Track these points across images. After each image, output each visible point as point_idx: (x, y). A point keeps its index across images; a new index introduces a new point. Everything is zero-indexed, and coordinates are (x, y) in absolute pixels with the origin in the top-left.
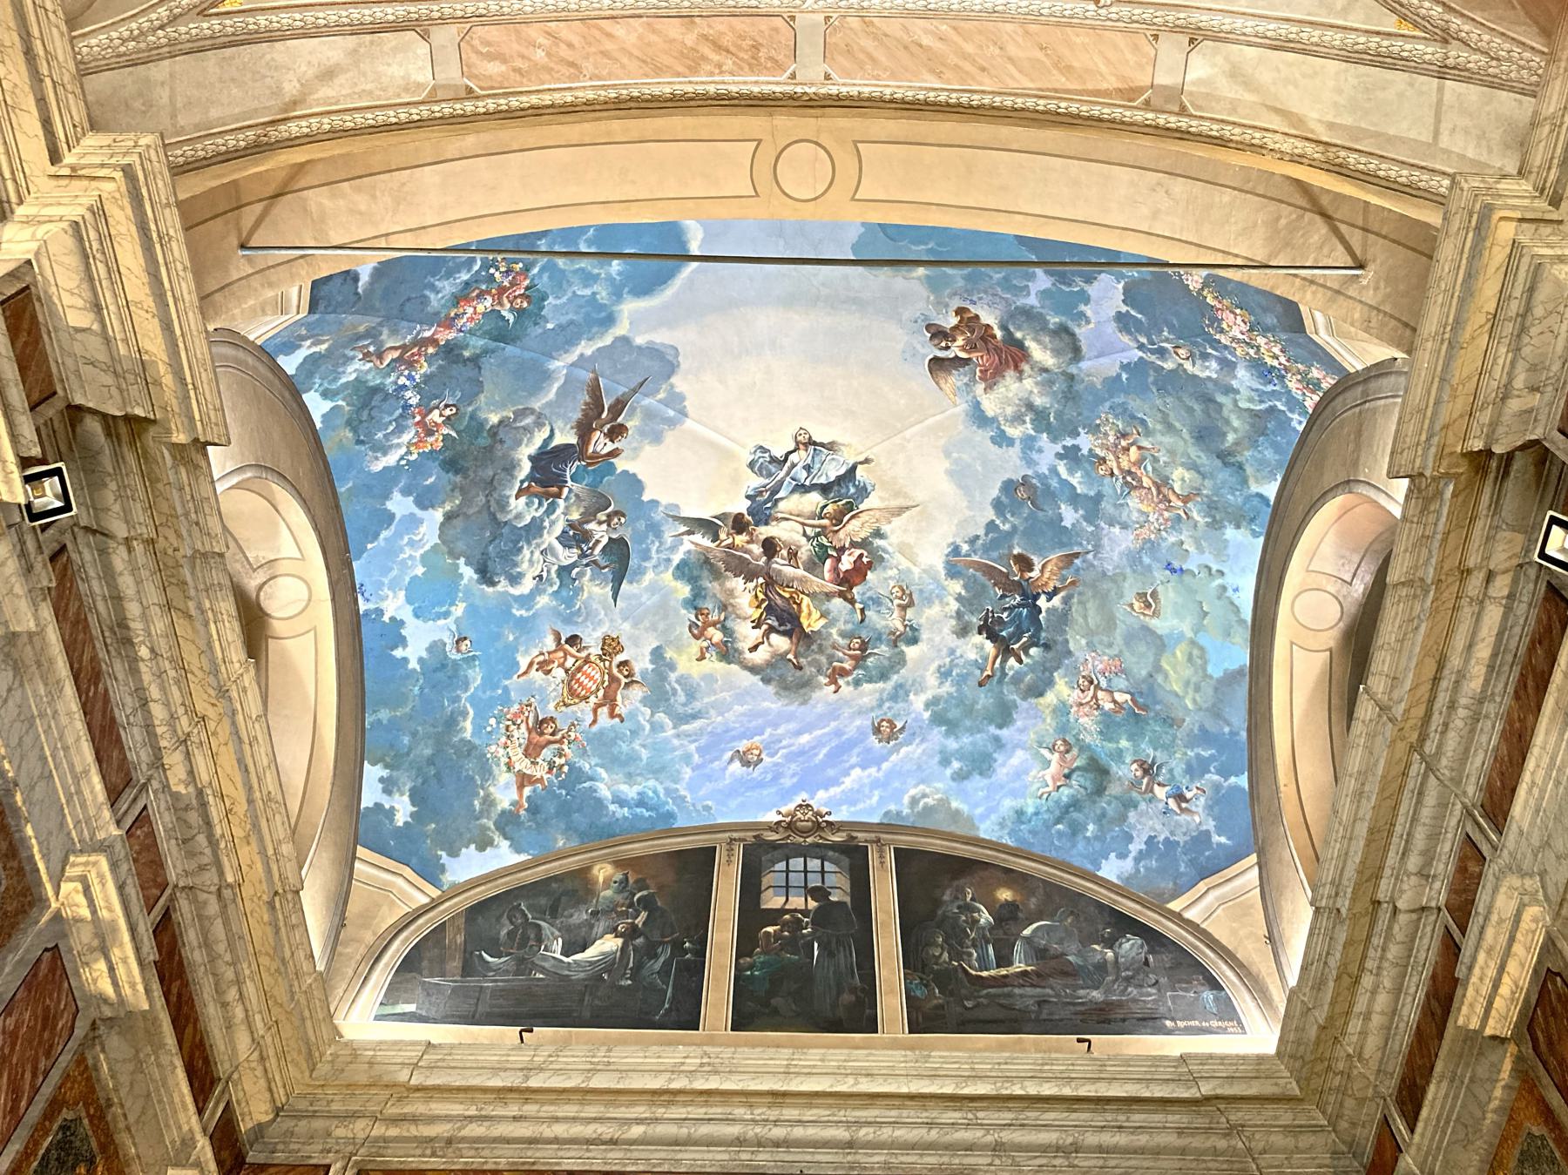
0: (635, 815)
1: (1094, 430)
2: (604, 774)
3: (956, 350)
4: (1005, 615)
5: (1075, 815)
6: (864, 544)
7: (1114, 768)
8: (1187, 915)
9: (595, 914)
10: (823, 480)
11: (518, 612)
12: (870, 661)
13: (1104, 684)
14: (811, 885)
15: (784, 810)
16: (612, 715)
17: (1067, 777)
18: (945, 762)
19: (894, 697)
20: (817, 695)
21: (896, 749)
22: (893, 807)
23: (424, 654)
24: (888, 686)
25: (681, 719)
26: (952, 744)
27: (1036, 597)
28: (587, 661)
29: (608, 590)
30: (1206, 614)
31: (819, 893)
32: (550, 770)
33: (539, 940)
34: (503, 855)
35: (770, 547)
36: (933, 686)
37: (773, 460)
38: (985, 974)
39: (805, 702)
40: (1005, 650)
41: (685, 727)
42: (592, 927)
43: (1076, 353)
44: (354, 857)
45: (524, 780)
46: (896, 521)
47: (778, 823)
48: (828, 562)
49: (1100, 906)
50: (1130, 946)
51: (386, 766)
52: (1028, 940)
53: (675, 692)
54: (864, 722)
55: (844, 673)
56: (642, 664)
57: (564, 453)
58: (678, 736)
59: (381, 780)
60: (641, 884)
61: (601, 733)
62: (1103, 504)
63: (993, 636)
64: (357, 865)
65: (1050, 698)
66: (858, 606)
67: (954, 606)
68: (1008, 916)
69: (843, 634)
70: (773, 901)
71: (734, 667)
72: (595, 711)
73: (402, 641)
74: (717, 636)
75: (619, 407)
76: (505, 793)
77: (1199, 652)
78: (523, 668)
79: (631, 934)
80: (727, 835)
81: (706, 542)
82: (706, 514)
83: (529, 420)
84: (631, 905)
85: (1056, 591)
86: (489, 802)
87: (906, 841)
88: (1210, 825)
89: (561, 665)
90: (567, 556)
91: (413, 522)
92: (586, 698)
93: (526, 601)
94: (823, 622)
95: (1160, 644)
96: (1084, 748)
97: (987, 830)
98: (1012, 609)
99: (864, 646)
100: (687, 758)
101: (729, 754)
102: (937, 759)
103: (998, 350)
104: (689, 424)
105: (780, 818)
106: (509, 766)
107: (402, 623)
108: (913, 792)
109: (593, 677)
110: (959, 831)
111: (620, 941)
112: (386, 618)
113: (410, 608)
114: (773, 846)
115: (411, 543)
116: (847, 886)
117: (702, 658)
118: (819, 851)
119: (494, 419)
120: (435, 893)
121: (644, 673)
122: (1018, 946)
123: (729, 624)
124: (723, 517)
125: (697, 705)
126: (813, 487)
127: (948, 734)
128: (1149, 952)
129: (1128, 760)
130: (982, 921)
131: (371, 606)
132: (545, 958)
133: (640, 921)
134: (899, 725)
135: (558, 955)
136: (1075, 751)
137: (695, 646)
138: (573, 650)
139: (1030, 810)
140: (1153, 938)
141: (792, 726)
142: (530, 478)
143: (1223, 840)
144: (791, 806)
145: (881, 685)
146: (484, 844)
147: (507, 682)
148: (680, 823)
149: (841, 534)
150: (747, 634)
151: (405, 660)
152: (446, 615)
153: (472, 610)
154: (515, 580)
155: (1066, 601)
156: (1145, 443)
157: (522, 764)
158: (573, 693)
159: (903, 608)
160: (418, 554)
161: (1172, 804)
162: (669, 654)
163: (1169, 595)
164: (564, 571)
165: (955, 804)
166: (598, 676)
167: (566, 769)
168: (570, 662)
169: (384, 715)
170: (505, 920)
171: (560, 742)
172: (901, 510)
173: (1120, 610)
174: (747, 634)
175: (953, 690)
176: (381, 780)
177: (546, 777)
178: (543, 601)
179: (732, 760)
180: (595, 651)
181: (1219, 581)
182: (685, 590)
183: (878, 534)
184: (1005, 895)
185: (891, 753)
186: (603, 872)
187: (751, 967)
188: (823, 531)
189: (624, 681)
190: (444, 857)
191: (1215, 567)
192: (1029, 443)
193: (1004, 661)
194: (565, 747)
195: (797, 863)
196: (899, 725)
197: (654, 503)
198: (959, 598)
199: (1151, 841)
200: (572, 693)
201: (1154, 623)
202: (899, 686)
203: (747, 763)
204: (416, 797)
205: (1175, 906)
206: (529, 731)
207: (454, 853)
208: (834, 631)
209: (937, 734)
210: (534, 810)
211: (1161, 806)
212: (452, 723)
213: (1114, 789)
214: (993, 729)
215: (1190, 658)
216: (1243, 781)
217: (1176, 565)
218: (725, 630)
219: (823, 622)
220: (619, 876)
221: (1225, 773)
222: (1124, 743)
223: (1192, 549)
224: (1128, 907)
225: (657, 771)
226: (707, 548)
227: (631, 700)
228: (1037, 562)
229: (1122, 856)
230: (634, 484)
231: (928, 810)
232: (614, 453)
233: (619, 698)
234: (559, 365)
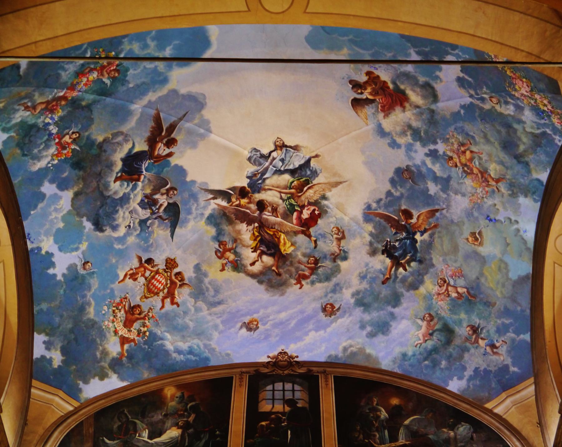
0: (187, 360)
1: (446, 141)
2: (168, 335)
3: (366, 95)
4: (397, 244)
5: (435, 356)
6: (316, 203)
7: (457, 329)
8: (496, 411)
9: (166, 416)
10: (291, 167)
11: (118, 246)
12: (320, 271)
13: (452, 283)
14: (287, 398)
15: (271, 355)
16: (173, 303)
17: (431, 335)
18: (363, 327)
19: (334, 291)
21: (335, 320)
22: (333, 353)
23: (65, 271)
24: (329, 285)
26: (367, 317)
27: (415, 234)
28: (157, 272)
29: (168, 232)
30: (508, 245)
31: (291, 402)
32: (138, 335)
33: (135, 431)
35: (261, 206)
36: (356, 284)
37: (262, 156)
39: (282, 294)
40: (397, 263)
41: (214, 310)
42: (164, 423)
43: (435, 97)
44: (31, 386)
45: (124, 340)
46: (334, 190)
47: (268, 363)
48: (295, 214)
49: (448, 407)
50: (463, 429)
51: (47, 334)
52: (407, 427)
53: (208, 289)
54: (317, 305)
55: (305, 277)
56: (189, 273)
57: (140, 157)
58: (210, 314)
59: (44, 342)
60: (191, 399)
61: (167, 314)
62: (452, 182)
63: (390, 256)
64: (33, 390)
65: (422, 290)
66: (313, 239)
67: (368, 238)
69: (304, 255)
71: (242, 275)
72: (163, 301)
73: (53, 265)
74: (232, 257)
75: (172, 128)
77: (503, 267)
78: (121, 278)
79: (185, 428)
80: (239, 370)
81: (224, 203)
82: (223, 187)
83: (120, 139)
84: (186, 410)
85: (426, 231)
86: (105, 353)
88: (509, 361)
89: (143, 275)
90: (144, 214)
91: (56, 198)
93: (121, 240)
94: (292, 248)
95: (483, 260)
96: (440, 318)
97: (386, 364)
98: (400, 240)
99: (316, 262)
100: (216, 327)
101: (239, 325)
102: (358, 325)
103: (391, 95)
104: (213, 136)
105: (269, 360)
106: (116, 332)
107: (52, 255)
108: (344, 344)
109: (161, 282)
110: (371, 366)
111: (180, 431)
112: (43, 252)
113: (56, 247)
114: (265, 376)
115: (56, 210)
116: (307, 399)
117: (223, 270)
118: (291, 379)
119: (100, 139)
120: (76, 404)
121: (190, 279)
122: (402, 431)
123: (238, 250)
124: (233, 189)
125: (220, 297)
126: (286, 171)
127: (364, 311)
128: (474, 432)
129: (465, 325)
130: (382, 417)
131: (34, 246)
132: (139, 441)
133: (191, 419)
134: (337, 307)
135: (146, 439)
136: (436, 320)
137: (219, 263)
138: (149, 267)
139: (410, 353)
140: (477, 425)
141: (275, 308)
142: (122, 170)
143: (516, 369)
144: (276, 353)
145: (326, 284)
146: (103, 376)
147: (112, 286)
148: (213, 363)
149: (303, 198)
150: (249, 255)
151: (55, 275)
152: (77, 249)
153: (91, 247)
154: (115, 228)
155: (431, 236)
156: (474, 149)
157: (123, 332)
158: (150, 291)
159: (339, 240)
160: (60, 216)
161: (488, 349)
162: (204, 268)
163: (488, 234)
164: (143, 222)
165: (368, 351)
166: (163, 281)
167: (147, 334)
168: (148, 274)
169: (44, 306)
170: (116, 419)
171: (144, 318)
172: (337, 184)
173: (461, 242)
174: (249, 255)
175: (367, 286)
176: (44, 342)
177: (136, 338)
178: (132, 240)
179: (241, 327)
180: (162, 267)
181: (515, 226)
182: (212, 231)
183: (324, 197)
184: (395, 401)
185: (332, 322)
186: (169, 391)
188: (292, 196)
189: (179, 283)
190: (81, 385)
191: (513, 218)
192: (409, 148)
193: (397, 269)
194: (147, 322)
195: (279, 386)
196: (337, 307)
197: (193, 182)
198: (371, 234)
199: (476, 370)
200: (150, 291)
201: (480, 249)
202: (337, 285)
203: (249, 329)
204: (64, 351)
205: (489, 406)
206: (126, 312)
207: (86, 382)
208: (299, 253)
209: (358, 312)
210: (130, 357)
211: (482, 351)
212: (82, 309)
213: (457, 341)
214: (390, 309)
215: (500, 269)
216: (527, 337)
217: (492, 217)
218: (236, 254)
219: (292, 248)
220: (179, 394)
221: (518, 332)
222: (463, 316)
223: (501, 209)
224: (463, 407)
225: (199, 334)
226: (224, 207)
228: (415, 214)
229: (460, 378)
230: (181, 171)
231: (353, 354)
232: (170, 155)
233: (176, 292)
234: (137, 107)
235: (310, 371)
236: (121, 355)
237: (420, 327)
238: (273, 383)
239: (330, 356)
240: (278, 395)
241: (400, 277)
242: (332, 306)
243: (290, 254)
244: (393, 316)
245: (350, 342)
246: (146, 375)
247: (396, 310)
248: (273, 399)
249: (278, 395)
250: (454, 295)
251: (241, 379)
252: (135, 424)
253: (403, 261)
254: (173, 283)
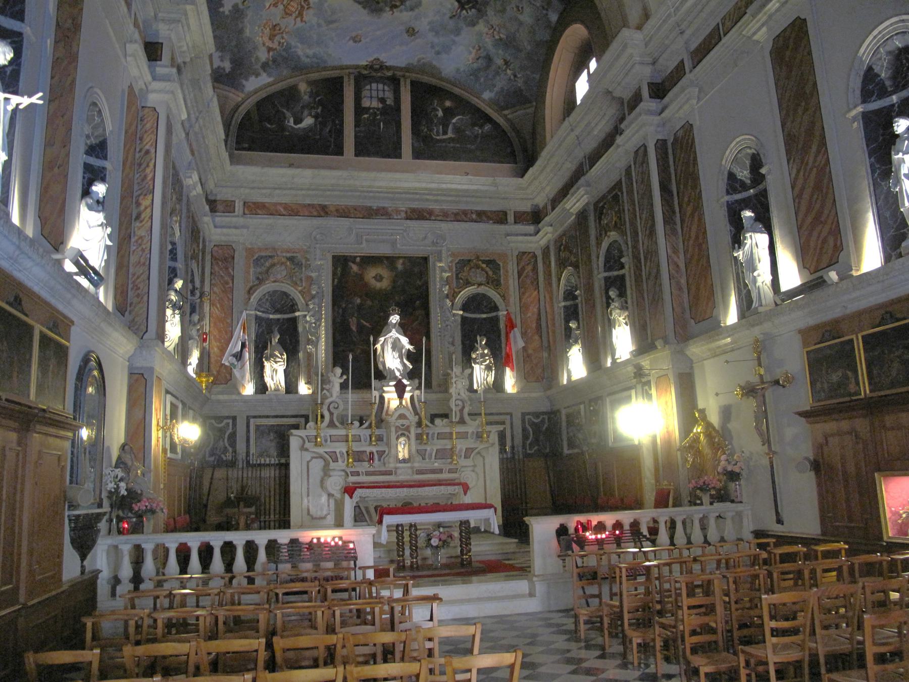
2: (299, 45)
13: (497, 29)
14: (380, 96)
16: (302, 21)
17: (478, 59)
20: (385, 15)
22: (411, 62)
26: (436, 40)
31: (382, 100)
32: (279, 45)
34: (264, 79)
38: (438, 138)
41: (331, 26)
42: (302, 113)
45: (269, 50)
47: (367, 65)
65: (477, 28)
68: (449, 113)
70: (366, 103)
72: (295, 19)
76: (263, 55)
79: (316, 117)
86: (257, 59)
87: (414, 76)
89: (282, 3)
92: (291, 15)
101: (348, 38)
102: (429, 46)
106: (264, 44)
108: (419, 57)
114: (365, 77)
116: (393, 98)
120: (243, 96)
122: (451, 127)
133: (319, 110)
135: (292, 124)
136: (482, 50)
144: (372, 59)
145: (410, 13)
146: (257, 75)
148: (330, 63)
157: (269, 44)
158: (287, 13)
161: (512, 77)
165: (434, 63)
167: (285, 44)
177: (278, 48)
179: (349, 40)
184: (448, 104)
186: (303, 87)
187: (360, 131)
189: (306, 7)
190: (244, 82)
194: (284, 35)
195: (374, 86)
203: (355, 42)
206: (270, 29)
207: (247, 80)
210: (274, 61)
212: (241, 31)
213: (494, 67)
220: (309, 90)
222: (500, 52)
231: (424, 64)
233: (304, 13)
235: (394, 75)
236: (268, 59)
237: (470, 53)
238: (370, 83)
239: (409, 64)
240: (374, 94)
241: (463, 16)
242: (413, 30)
244: (454, 42)
245: (423, 56)
246: (285, 72)
247: (457, 39)
248: (371, 97)
249: (374, 94)
250: (497, 37)
251: (349, 78)
252: (284, 113)
253: (467, 7)
254: (302, 7)
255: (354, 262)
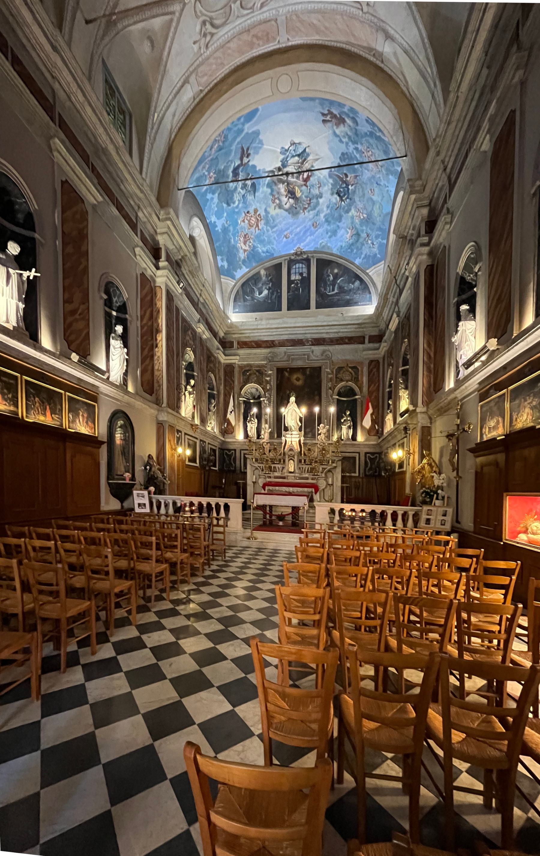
25: (272, 228)
71: (282, 210)
148: (275, 255)
198: (332, 184)
225: (270, 242)
227: (261, 225)
243: (300, 197)
255: (287, 371)
